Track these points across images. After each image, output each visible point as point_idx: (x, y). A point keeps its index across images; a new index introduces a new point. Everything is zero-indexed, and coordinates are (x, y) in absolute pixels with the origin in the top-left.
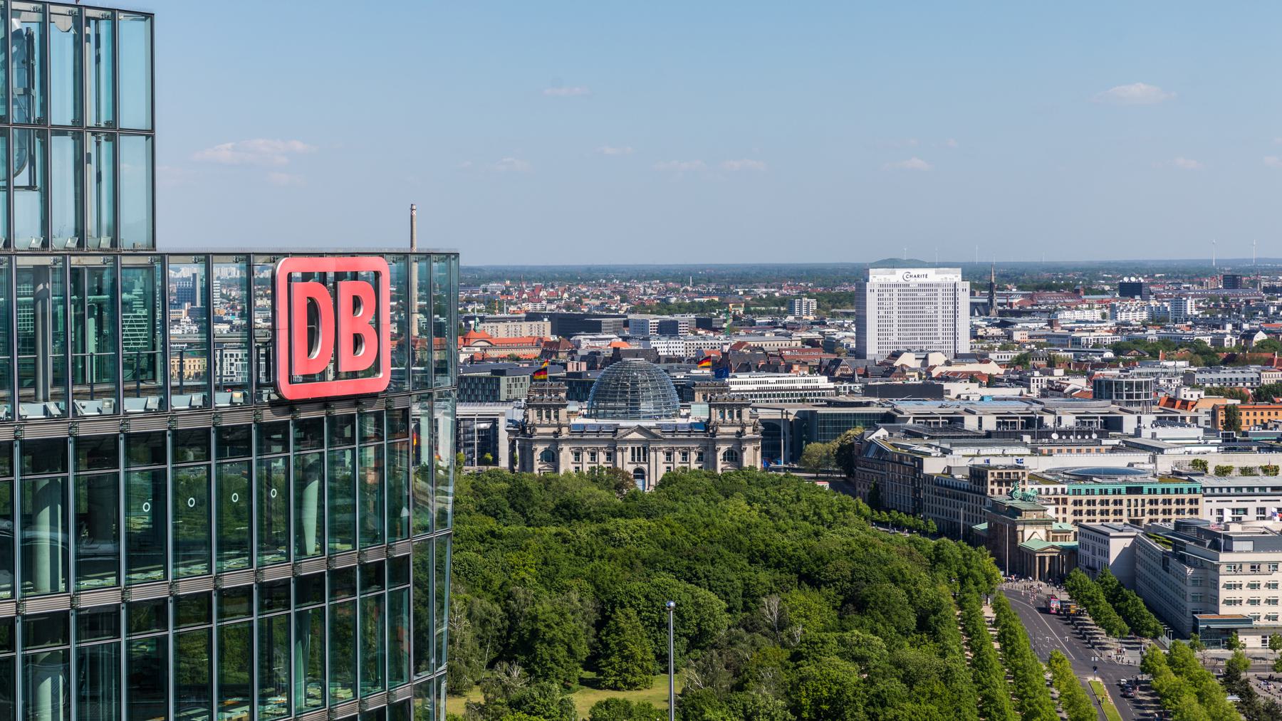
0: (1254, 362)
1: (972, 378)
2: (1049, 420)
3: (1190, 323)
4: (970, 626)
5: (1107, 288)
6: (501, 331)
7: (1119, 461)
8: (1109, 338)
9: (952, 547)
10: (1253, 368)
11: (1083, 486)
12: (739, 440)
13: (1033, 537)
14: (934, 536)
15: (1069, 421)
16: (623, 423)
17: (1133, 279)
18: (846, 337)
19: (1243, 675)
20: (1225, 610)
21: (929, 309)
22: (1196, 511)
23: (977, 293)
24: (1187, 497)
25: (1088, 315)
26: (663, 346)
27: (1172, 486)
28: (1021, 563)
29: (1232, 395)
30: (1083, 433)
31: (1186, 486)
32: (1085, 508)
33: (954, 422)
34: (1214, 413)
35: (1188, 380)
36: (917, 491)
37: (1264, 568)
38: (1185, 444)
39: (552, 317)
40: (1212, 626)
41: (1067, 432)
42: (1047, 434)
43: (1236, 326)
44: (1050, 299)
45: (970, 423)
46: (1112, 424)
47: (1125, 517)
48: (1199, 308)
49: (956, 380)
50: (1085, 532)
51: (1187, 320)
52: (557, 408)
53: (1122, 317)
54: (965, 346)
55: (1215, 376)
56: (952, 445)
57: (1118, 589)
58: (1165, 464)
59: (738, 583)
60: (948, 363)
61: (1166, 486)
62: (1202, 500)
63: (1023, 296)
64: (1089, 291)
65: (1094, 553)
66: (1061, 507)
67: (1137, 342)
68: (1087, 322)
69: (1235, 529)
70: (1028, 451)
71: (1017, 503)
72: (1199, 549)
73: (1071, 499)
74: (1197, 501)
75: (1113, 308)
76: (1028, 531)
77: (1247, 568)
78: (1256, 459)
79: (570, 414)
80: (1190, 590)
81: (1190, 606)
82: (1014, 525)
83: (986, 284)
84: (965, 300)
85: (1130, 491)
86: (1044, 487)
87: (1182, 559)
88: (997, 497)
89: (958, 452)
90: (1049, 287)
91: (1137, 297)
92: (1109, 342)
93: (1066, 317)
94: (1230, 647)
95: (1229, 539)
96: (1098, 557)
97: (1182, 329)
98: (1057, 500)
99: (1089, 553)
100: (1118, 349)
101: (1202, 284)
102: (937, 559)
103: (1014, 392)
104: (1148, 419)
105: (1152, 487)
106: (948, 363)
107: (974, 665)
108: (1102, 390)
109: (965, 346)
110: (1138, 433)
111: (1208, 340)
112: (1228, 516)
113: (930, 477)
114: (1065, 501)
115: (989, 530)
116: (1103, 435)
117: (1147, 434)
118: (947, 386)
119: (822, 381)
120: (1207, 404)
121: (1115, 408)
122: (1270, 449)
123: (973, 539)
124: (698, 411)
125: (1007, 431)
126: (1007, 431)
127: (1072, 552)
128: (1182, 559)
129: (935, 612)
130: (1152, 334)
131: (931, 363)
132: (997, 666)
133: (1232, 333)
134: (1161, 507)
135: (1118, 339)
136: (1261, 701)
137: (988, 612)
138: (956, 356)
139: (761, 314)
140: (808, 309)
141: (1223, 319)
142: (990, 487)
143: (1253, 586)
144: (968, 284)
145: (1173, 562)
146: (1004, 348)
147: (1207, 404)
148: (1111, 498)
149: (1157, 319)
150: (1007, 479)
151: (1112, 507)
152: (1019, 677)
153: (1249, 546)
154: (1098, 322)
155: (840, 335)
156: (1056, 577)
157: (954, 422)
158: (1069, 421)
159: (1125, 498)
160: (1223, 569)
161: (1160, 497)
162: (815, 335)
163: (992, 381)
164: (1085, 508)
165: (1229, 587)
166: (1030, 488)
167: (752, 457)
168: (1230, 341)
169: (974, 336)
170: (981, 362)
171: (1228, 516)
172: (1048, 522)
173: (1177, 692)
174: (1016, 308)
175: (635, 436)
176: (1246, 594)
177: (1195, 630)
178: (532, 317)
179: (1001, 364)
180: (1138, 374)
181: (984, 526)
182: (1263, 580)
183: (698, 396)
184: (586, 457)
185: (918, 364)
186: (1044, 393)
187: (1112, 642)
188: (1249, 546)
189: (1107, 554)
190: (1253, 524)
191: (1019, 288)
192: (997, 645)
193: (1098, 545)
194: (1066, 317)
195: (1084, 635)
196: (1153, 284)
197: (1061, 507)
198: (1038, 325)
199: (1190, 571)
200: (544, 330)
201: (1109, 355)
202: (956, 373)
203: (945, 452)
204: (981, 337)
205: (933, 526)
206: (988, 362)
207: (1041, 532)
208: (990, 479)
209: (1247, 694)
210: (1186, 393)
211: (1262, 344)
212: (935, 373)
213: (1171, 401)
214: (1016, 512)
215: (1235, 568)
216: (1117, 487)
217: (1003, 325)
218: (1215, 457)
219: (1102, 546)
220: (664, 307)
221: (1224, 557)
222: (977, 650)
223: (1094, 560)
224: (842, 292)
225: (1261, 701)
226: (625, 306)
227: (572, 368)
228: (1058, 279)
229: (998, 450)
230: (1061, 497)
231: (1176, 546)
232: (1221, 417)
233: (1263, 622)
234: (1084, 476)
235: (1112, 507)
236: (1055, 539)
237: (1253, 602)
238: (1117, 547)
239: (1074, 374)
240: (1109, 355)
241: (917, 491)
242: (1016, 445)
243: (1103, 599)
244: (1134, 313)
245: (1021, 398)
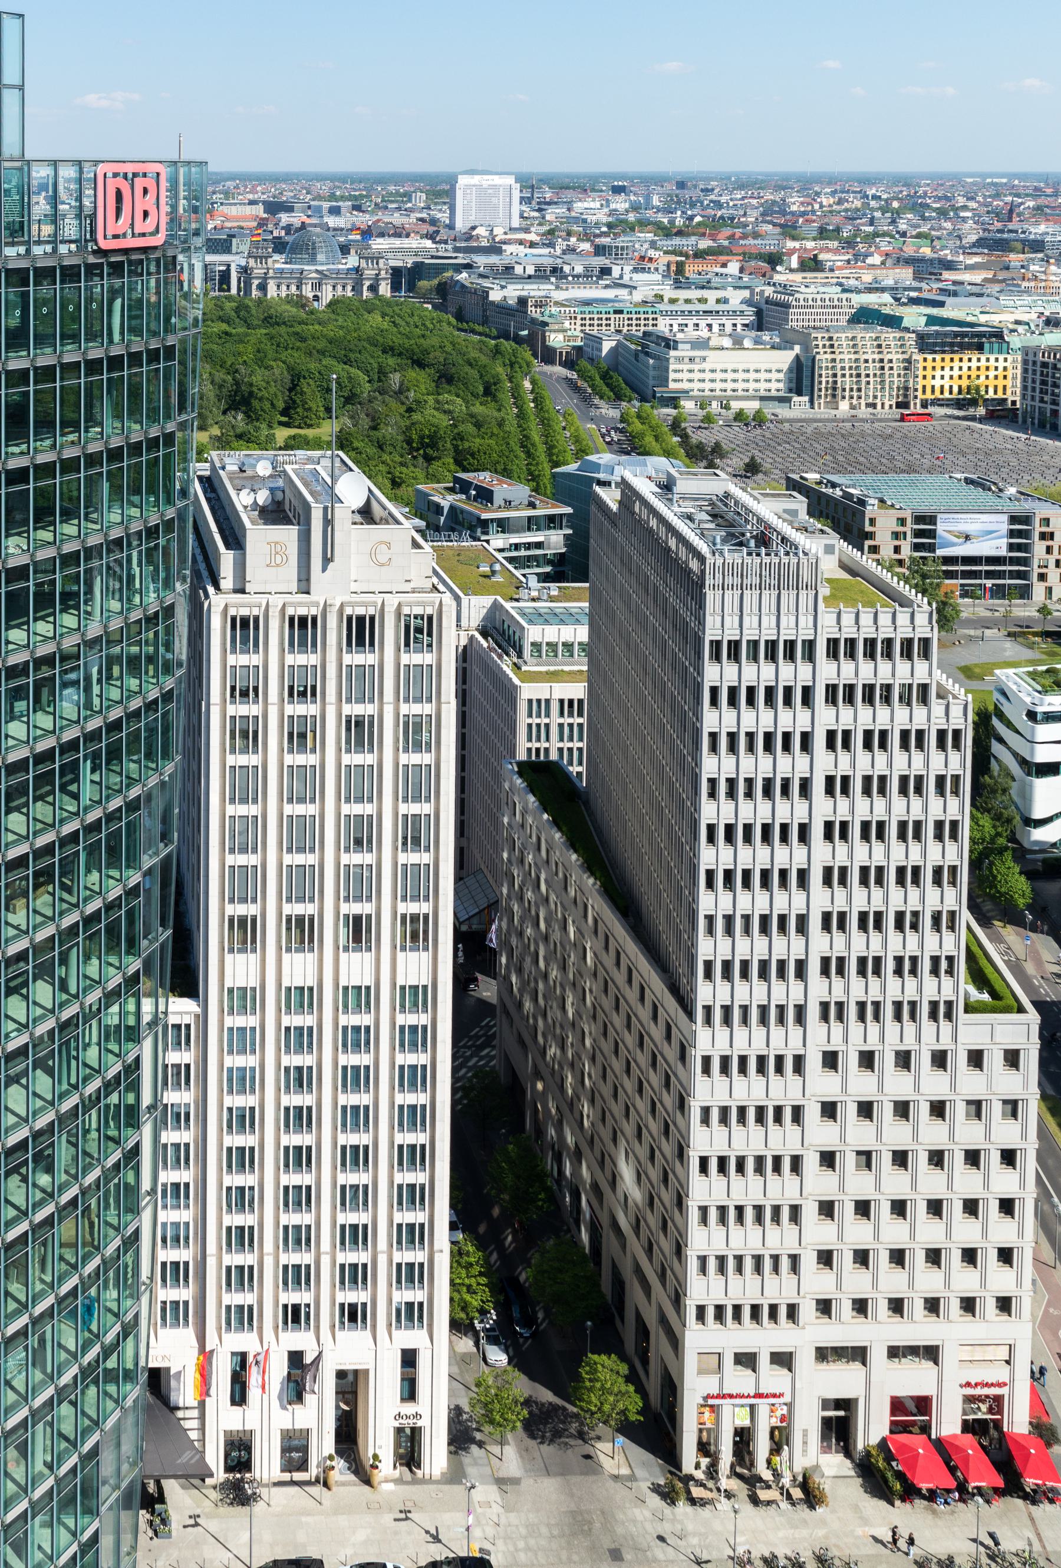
0: (694, 234)
1: (521, 242)
2: (567, 269)
4: (516, 393)
6: (233, 211)
7: (610, 294)
8: (605, 219)
9: (507, 345)
10: (693, 238)
11: (587, 309)
12: (377, 279)
13: (555, 340)
14: (494, 338)
15: (579, 269)
16: (306, 268)
18: (444, 217)
19: (683, 425)
20: (672, 385)
21: (494, 200)
24: (651, 316)
25: (592, 205)
26: (332, 221)
27: (642, 310)
28: (548, 356)
29: (681, 254)
30: (587, 277)
31: (650, 310)
32: (588, 322)
33: (509, 269)
34: (668, 265)
35: (653, 245)
36: (485, 311)
37: (697, 360)
38: (650, 284)
39: (264, 203)
41: (578, 276)
42: (566, 277)
44: (568, 195)
45: (518, 270)
46: (605, 271)
47: (612, 328)
50: (588, 337)
52: (266, 258)
53: (613, 206)
54: (516, 223)
55: (669, 243)
57: (607, 372)
58: (637, 296)
59: (376, 365)
62: (660, 318)
64: (593, 190)
67: (622, 221)
69: (680, 336)
71: (546, 319)
72: (657, 348)
73: (579, 317)
75: (608, 201)
76: (553, 336)
77: (686, 360)
78: (694, 294)
79: (275, 261)
80: (652, 373)
81: (651, 382)
82: (544, 332)
83: (529, 185)
84: (516, 195)
85: (615, 312)
87: (647, 354)
88: (534, 315)
89: (510, 287)
90: (568, 188)
93: (579, 206)
94: (675, 408)
95: (676, 342)
97: (649, 214)
100: (610, 226)
102: (497, 352)
103: (545, 251)
104: (628, 269)
107: (518, 416)
108: (600, 250)
109: (516, 223)
110: (621, 277)
111: (666, 221)
112: (676, 328)
113: (493, 303)
116: (599, 278)
117: (626, 277)
118: (504, 247)
119: (428, 243)
120: (665, 259)
121: (607, 262)
122: (703, 288)
123: (518, 340)
124: (352, 261)
125: (541, 275)
126: (541, 275)
127: (579, 349)
128: (647, 354)
129: (495, 384)
130: (631, 217)
132: (532, 417)
134: (634, 322)
135: (610, 219)
136: (694, 441)
137: (527, 385)
139: (392, 202)
140: (420, 199)
143: (690, 371)
145: (641, 356)
146: (540, 224)
147: (665, 259)
148: (604, 316)
149: (635, 208)
150: (539, 305)
151: (604, 322)
152: (545, 423)
153: (688, 346)
155: (439, 215)
156: (569, 363)
157: (509, 269)
158: (579, 269)
159: (612, 316)
160: (672, 360)
161: (634, 316)
162: (424, 215)
163: (532, 245)
164: (588, 322)
165: (675, 371)
166: (554, 310)
167: (385, 289)
168: (679, 222)
169: (522, 217)
171: (676, 328)
172: (565, 331)
173: (642, 435)
175: (314, 275)
176: (686, 376)
177: (654, 397)
178: (252, 203)
179: (538, 234)
180: (622, 241)
181: (526, 332)
182: (696, 367)
183: (353, 252)
184: (284, 288)
185: (487, 234)
186: (564, 252)
187: (602, 403)
188: (688, 346)
189: (601, 350)
190: (691, 333)
192: (532, 405)
194: (579, 206)
195: (586, 400)
198: (561, 210)
199: (651, 361)
200: (259, 210)
201: (604, 229)
203: (503, 287)
205: (494, 332)
207: (560, 337)
209: (685, 437)
210: (652, 253)
211: (699, 224)
212: (497, 239)
213: (642, 258)
214: (546, 324)
215: (680, 360)
217: (540, 210)
218: (668, 292)
220: (332, 197)
221: (672, 353)
222: (520, 408)
224: (442, 190)
225: (694, 441)
226: (309, 197)
227: (276, 234)
229: (535, 287)
231: (644, 346)
232: (673, 268)
233: (696, 393)
234: (587, 303)
235: (604, 322)
237: (690, 381)
238: (607, 346)
239: (583, 240)
240: (604, 229)
241: (485, 311)
243: (597, 378)
244: (620, 204)
245: (550, 256)
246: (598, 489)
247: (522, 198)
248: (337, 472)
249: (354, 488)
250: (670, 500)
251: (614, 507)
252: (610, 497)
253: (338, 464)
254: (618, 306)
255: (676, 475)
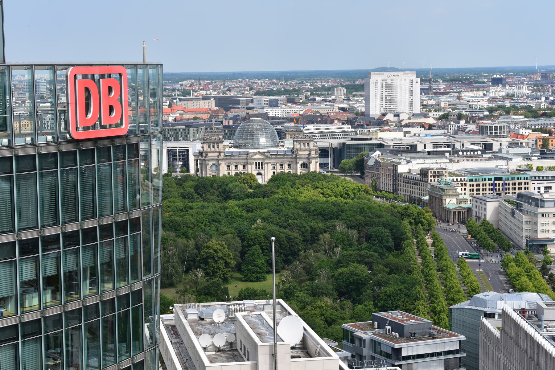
1: (422, 125)
2: (458, 146)
3: (525, 97)
5: (486, 80)
6: (190, 105)
7: (492, 165)
8: (486, 105)
11: (474, 177)
12: (309, 157)
16: (251, 151)
17: (498, 76)
18: (360, 106)
22: (528, 188)
23: (423, 83)
26: (272, 112)
28: (446, 215)
31: (523, 176)
39: (215, 98)
40: (535, 243)
43: (547, 99)
45: (420, 148)
46: (488, 147)
48: (529, 90)
49: (413, 127)
51: (523, 95)
52: (218, 143)
54: (417, 110)
55: (537, 123)
56: (411, 158)
58: (513, 166)
59: (308, 228)
60: (409, 118)
61: (513, 176)
62: (530, 183)
63: (445, 84)
65: (479, 210)
66: (463, 188)
67: (500, 107)
68: (476, 97)
69: (546, 196)
70: (448, 161)
71: (442, 186)
73: (468, 184)
74: (528, 183)
79: (225, 146)
82: (441, 196)
84: (417, 87)
86: (455, 178)
88: (433, 183)
89: (414, 162)
91: (500, 85)
92: (486, 107)
95: (542, 201)
96: (481, 212)
98: (462, 184)
99: (477, 210)
100: (491, 110)
101: (530, 78)
104: (505, 144)
105: (507, 177)
106: (409, 118)
108: (482, 130)
109: (417, 110)
110: (500, 151)
112: (542, 190)
113: (401, 175)
114: (465, 185)
115: (430, 199)
117: (504, 151)
119: (349, 128)
124: (288, 144)
131: (401, 119)
133: (545, 102)
135: (491, 105)
138: (413, 115)
139: (319, 95)
140: (340, 92)
141: (541, 95)
142: (430, 178)
144: (419, 79)
154: (482, 97)
155: (356, 105)
162: (345, 105)
163: (431, 127)
165: (543, 224)
167: (314, 167)
170: (425, 117)
171: (542, 190)
174: (442, 91)
175: (258, 156)
178: (205, 98)
179: (435, 119)
181: (427, 198)
183: (288, 136)
184: (233, 167)
186: (456, 133)
189: (485, 210)
191: (444, 81)
193: (481, 205)
196: (507, 78)
197: (463, 188)
200: (211, 104)
201: (487, 113)
202: (413, 123)
203: (408, 162)
204: (426, 105)
206: (429, 117)
207: (454, 200)
208: (430, 174)
210: (522, 131)
214: (443, 190)
216: (490, 177)
218: (536, 162)
219: (484, 206)
220: (270, 93)
221: (541, 210)
223: (479, 213)
224: (357, 85)
226: (252, 92)
227: (225, 123)
228: (463, 77)
229: (433, 161)
230: (463, 183)
232: (540, 142)
236: (460, 203)
240: (487, 113)
242: (442, 158)
244: (498, 92)
245: (446, 135)
246: (484, 320)
247: (422, 90)
248: (278, 315)
249: (293, 328)
250: (539, 326)
251: (497, 333)
252: (493, 326)
253: (278, 309)
254: (498, 175)
255: (544, 306)
